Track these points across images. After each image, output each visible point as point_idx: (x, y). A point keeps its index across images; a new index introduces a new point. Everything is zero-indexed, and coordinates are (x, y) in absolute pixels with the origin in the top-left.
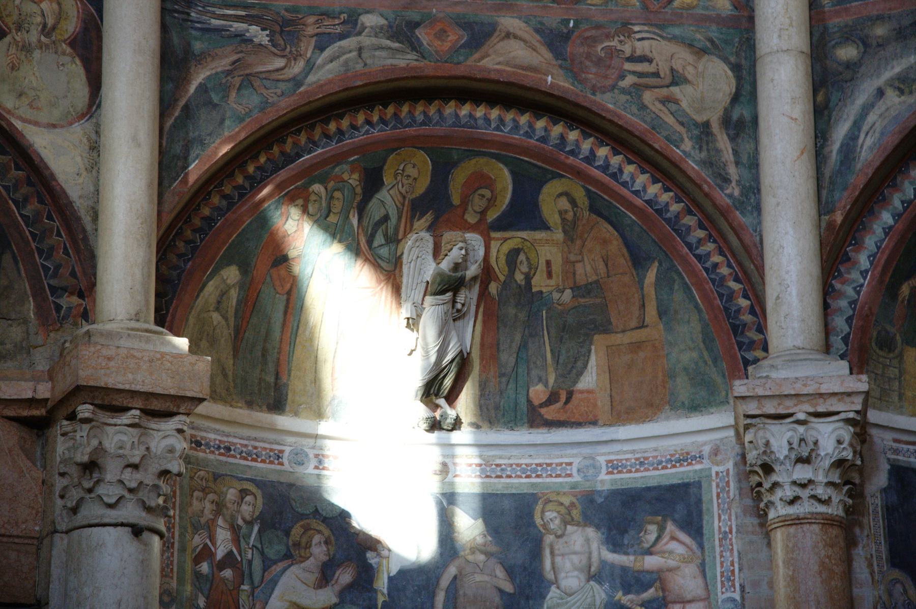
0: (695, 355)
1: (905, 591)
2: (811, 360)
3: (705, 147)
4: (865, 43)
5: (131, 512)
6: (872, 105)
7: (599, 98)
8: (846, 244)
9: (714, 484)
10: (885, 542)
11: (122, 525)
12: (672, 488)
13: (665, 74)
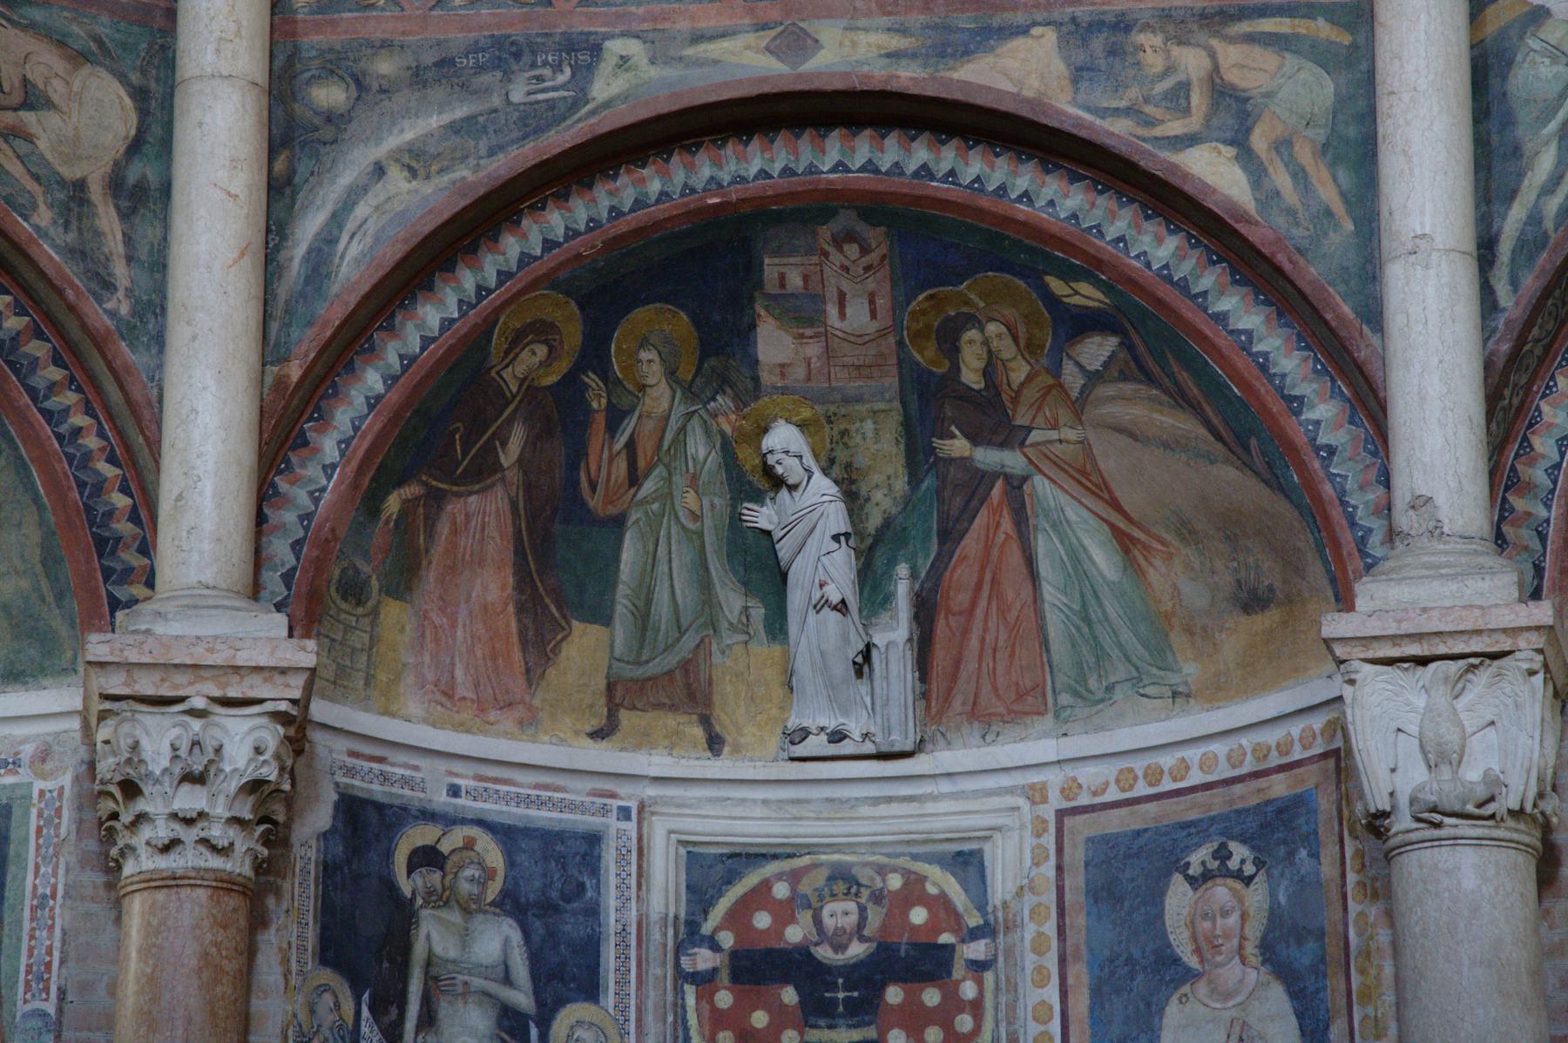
0: (24, 583)
1: (337, 1005)
2: (227, 608)
3: (74, 225)
4: (359, 82)
6: (365, 189)
8: (305, 417)
9: (34, 811)
10: (315, 922)
13: (12, 86)
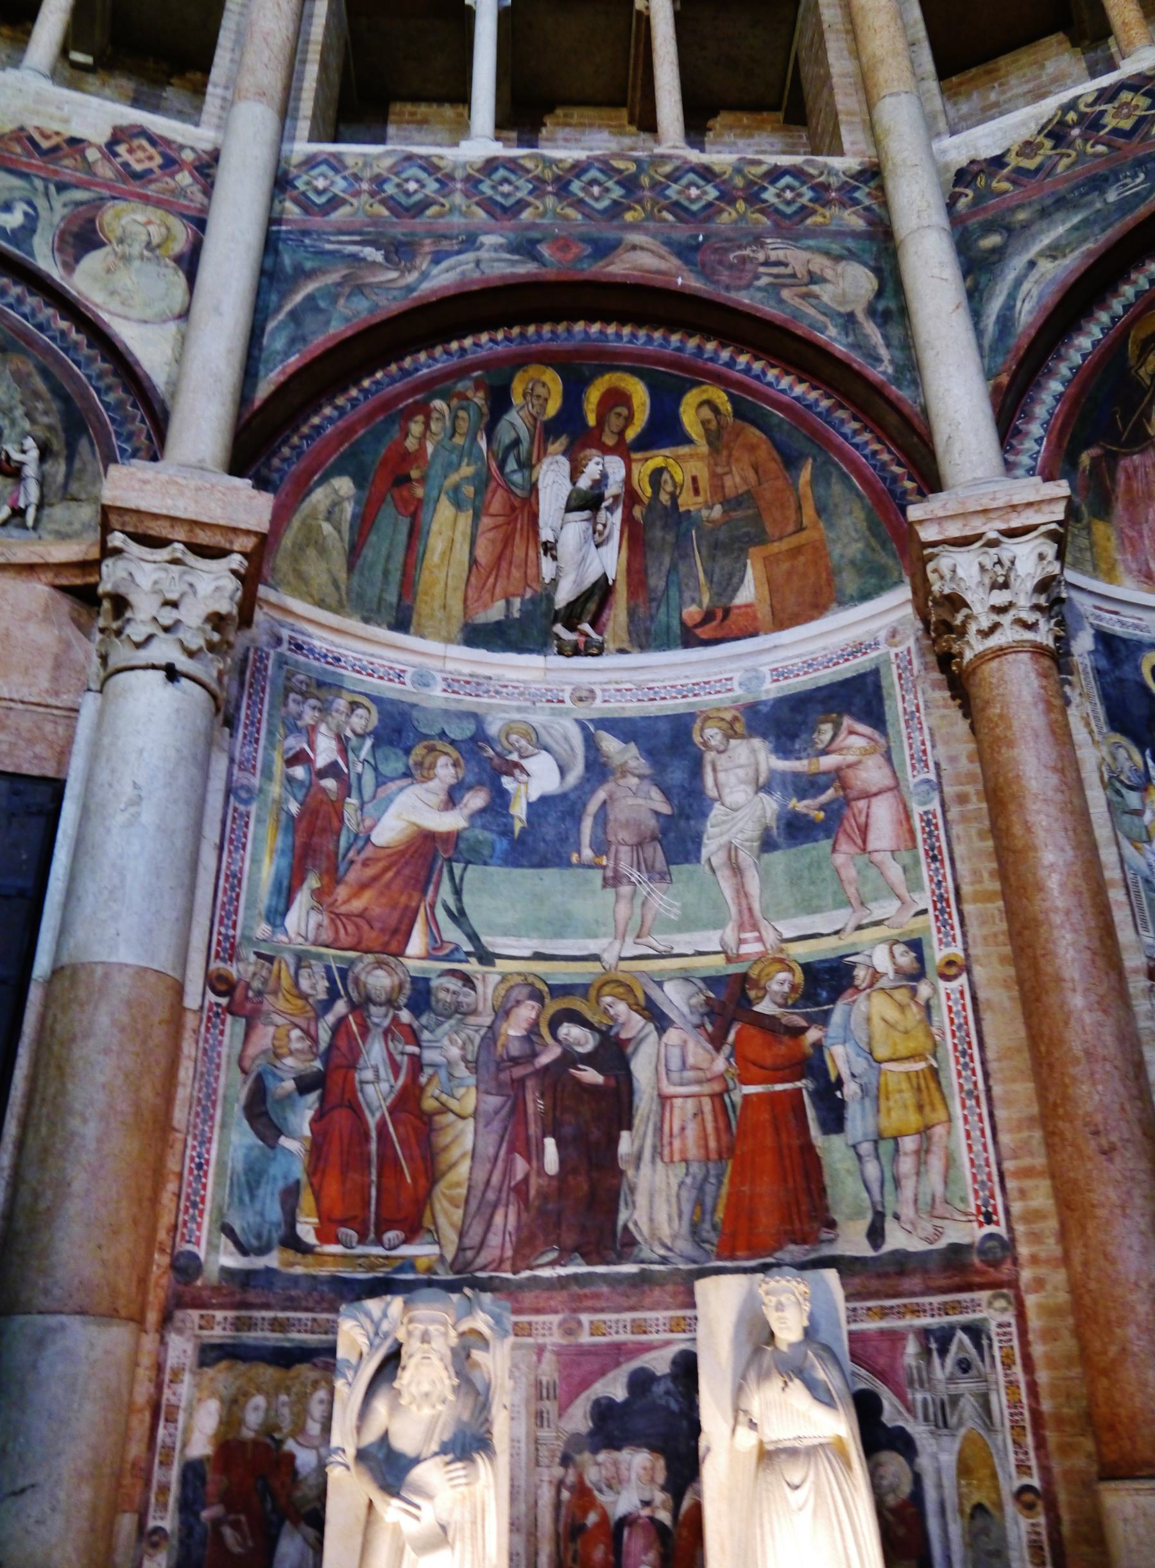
1: (1130, 758)
4: (1009, 230)
5: (164, 651)
6: (1026, 276)
7: (733, 295)
11: (154, 667)
12: (845, 683)
